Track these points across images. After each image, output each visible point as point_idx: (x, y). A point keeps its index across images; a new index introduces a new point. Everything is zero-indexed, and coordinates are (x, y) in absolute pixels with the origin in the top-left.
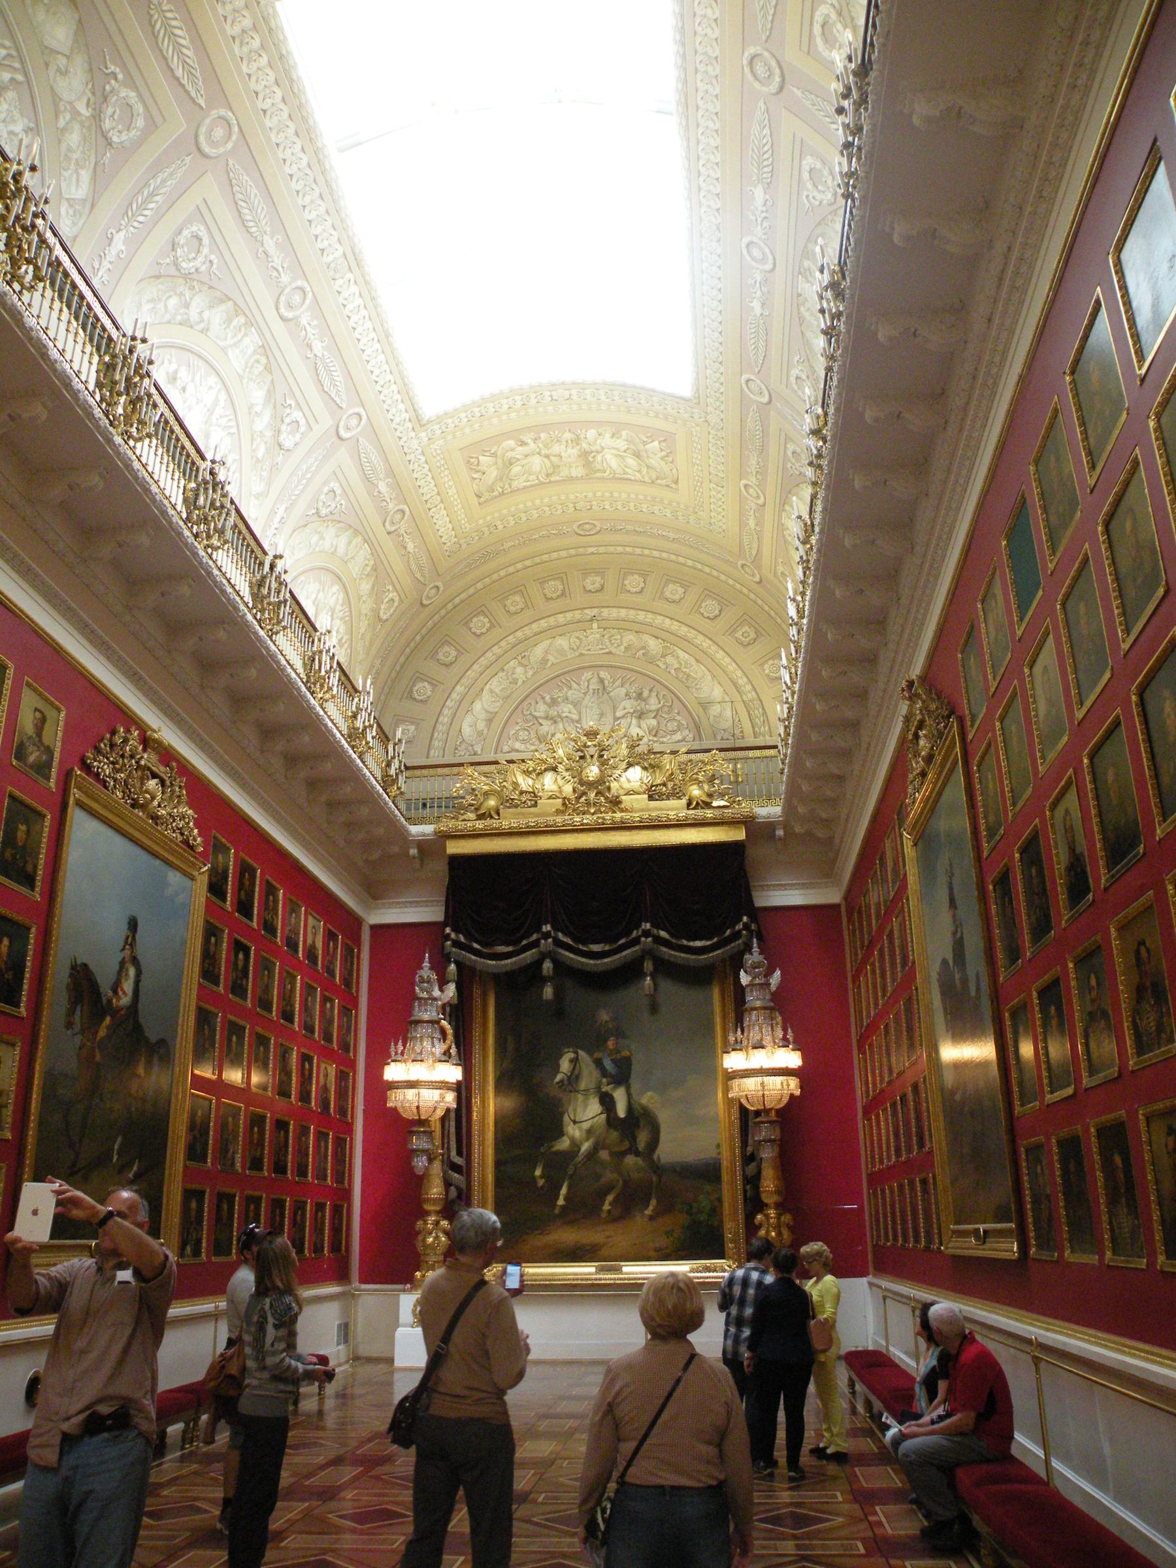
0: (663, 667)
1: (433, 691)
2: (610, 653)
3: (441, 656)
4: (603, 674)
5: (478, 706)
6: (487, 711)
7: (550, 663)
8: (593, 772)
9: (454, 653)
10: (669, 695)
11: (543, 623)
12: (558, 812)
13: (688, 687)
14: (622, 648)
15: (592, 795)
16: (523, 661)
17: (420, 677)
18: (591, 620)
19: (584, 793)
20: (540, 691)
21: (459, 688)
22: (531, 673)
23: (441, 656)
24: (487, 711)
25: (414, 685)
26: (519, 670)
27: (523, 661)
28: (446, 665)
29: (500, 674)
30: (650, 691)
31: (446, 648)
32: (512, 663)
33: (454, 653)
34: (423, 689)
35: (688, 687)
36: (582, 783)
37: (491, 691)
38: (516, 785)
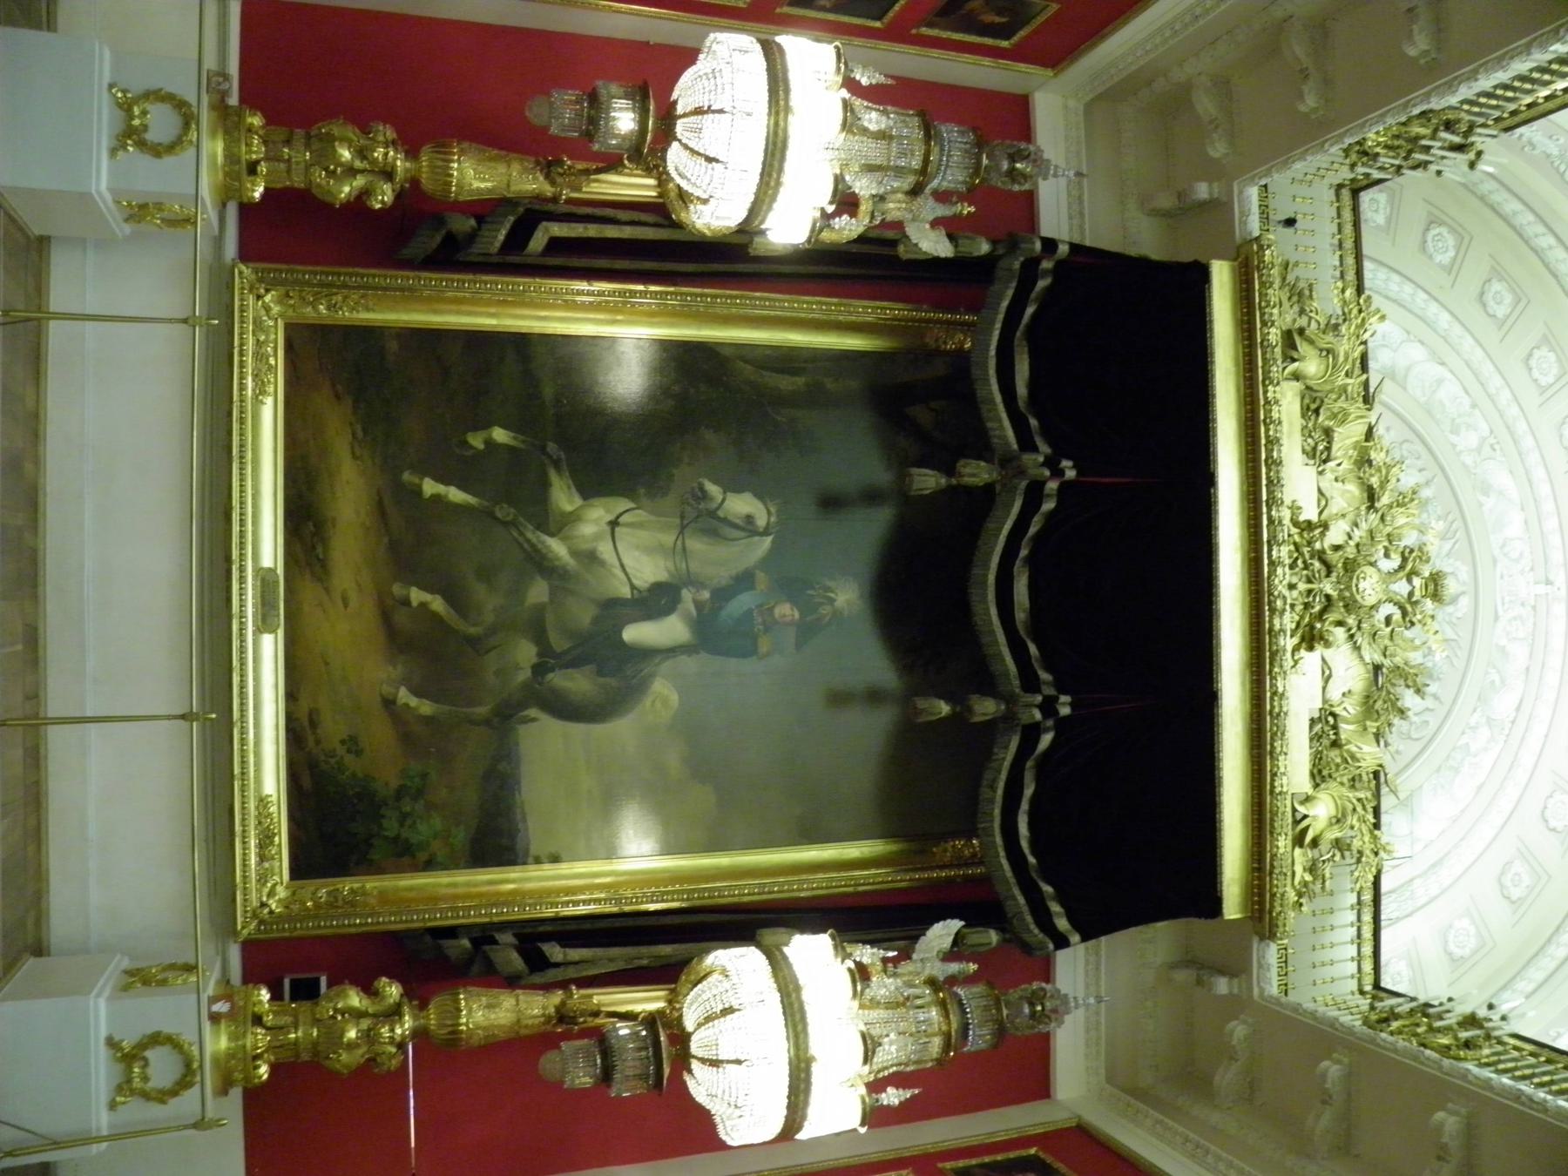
0: (1473, 722)
1: (1441, 266)
2: (1497, 618)
3: (1497, 286)
4: (1464, 602)
5: (1416, 352)
6: (1408, 369)
7: (1482, 499)
8: (1369, 587)
9: (1501, 311)
10: (1428, 732)
11: (1544, 490)
12: (1295, 509)
13: (1438, 770)
14: (1503, 642)
15: (1328, 587)
16: (1487, 449)
17: (1463, 240)
18: (1548, 582)
19: (1329, 569)
20: (1440, 479)
21: (1445, 317)
22: (1469, 460)
23: (1497, 286)
24: (1408, 369)
25: (1452, 230)
26: (1472, 440)
27: (1487, 449)
28: (1482, 294)
29: (1466, 401)
30: (1436, 697)
31: (1508, 299)
32: (1484, 427)
33: (1501, 311)
34: (1444, 246)
35: (1438, 770)
36: (1350, 567)
37: (1440, 382)
38: (1342, 417)
